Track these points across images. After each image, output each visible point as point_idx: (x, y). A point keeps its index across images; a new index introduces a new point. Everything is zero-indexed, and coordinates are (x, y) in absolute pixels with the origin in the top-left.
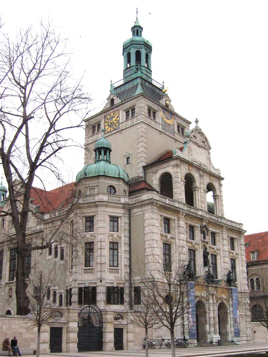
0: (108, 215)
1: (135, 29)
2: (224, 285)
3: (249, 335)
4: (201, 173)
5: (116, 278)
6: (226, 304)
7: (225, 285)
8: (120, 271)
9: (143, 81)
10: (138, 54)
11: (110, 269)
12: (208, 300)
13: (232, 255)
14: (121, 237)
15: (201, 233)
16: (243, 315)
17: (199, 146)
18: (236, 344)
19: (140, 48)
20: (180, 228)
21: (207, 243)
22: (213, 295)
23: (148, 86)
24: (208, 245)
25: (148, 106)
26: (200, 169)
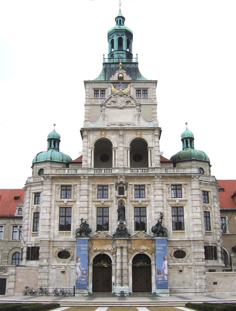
0: (33, 193)
1: (119, 19)
2: (144, 237)
3: (198, 287)
4: (121, 133)
5: (36, 239)
6: (149, 255)
7: (145, 236)
8: (39, 234)
10: (120, 40)
11: (32, 233)
13: (175, 203)
14: (40, 208)
15: (116, 190)
16: (192, 265)
17: (121, 108)
18: (158, 296)
19: (113, 37)
20: (82, 191)
21: (125, 198)
22: (122, 248)
24: (128, 200)
25: (94, 89)
26: (118, 129)
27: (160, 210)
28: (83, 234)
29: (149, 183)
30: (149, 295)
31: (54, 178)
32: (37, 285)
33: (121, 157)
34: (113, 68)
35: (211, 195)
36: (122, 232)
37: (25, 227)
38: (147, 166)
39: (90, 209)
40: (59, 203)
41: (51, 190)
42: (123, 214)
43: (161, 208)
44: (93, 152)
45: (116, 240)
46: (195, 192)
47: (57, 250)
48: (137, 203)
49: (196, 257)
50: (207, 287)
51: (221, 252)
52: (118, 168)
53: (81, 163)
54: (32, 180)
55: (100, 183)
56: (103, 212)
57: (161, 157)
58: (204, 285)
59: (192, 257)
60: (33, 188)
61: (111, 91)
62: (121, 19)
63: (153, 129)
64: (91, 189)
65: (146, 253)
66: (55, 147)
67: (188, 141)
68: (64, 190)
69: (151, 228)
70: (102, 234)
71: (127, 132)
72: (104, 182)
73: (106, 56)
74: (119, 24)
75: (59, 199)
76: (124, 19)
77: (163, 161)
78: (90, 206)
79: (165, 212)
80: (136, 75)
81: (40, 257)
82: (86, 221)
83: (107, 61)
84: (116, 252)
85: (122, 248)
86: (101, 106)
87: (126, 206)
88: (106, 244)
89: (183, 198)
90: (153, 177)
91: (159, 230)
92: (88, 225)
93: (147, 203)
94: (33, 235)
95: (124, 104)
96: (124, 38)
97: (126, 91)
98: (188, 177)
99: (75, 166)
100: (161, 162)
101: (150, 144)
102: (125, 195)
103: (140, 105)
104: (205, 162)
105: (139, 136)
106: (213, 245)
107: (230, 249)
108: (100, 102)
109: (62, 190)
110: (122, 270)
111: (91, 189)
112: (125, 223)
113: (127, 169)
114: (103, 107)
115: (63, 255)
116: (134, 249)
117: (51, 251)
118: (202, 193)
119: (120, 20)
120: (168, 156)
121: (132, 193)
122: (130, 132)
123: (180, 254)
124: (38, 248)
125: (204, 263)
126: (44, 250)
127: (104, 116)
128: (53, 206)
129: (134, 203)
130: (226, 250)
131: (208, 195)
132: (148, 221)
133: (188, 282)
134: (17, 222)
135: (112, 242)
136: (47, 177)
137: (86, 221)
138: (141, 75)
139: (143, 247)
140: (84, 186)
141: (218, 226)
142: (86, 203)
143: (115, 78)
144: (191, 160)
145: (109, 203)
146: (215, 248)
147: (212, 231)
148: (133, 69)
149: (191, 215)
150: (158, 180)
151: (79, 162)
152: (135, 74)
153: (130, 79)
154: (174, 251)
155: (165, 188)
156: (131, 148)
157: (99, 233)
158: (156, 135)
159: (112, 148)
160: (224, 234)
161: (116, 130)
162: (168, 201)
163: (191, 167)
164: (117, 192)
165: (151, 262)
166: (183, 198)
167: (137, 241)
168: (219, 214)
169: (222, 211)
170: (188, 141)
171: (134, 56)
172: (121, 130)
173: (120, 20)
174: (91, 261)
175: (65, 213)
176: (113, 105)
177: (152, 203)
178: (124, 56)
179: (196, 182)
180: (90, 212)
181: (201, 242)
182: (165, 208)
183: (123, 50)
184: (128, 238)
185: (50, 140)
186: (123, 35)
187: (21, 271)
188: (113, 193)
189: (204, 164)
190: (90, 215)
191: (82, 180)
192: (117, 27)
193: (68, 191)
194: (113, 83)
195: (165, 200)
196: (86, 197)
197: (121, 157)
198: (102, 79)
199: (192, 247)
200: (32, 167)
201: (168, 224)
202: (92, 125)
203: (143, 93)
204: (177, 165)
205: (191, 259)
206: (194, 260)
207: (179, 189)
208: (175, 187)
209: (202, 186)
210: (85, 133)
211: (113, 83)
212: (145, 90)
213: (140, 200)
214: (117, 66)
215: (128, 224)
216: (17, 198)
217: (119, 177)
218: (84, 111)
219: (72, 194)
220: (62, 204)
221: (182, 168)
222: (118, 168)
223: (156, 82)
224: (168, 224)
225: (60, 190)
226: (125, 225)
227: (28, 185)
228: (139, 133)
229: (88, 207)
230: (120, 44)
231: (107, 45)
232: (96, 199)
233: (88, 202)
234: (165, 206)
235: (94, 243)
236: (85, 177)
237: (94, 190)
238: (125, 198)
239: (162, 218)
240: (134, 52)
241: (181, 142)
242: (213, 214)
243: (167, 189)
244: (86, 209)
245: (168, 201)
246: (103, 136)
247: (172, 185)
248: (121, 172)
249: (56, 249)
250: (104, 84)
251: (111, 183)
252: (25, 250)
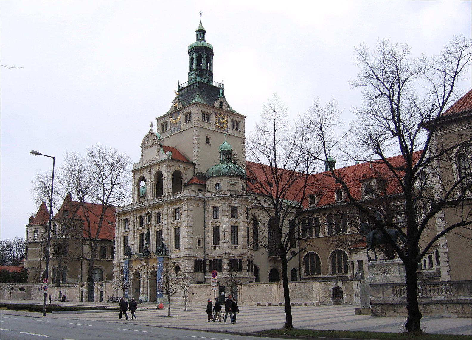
17: (150, 147)
22: (144, 266)
29: (162, 210)
106: (219, 258)
119: (201, 33)
159: (162, 179)
173: (201, 33)
180: (135, 239)
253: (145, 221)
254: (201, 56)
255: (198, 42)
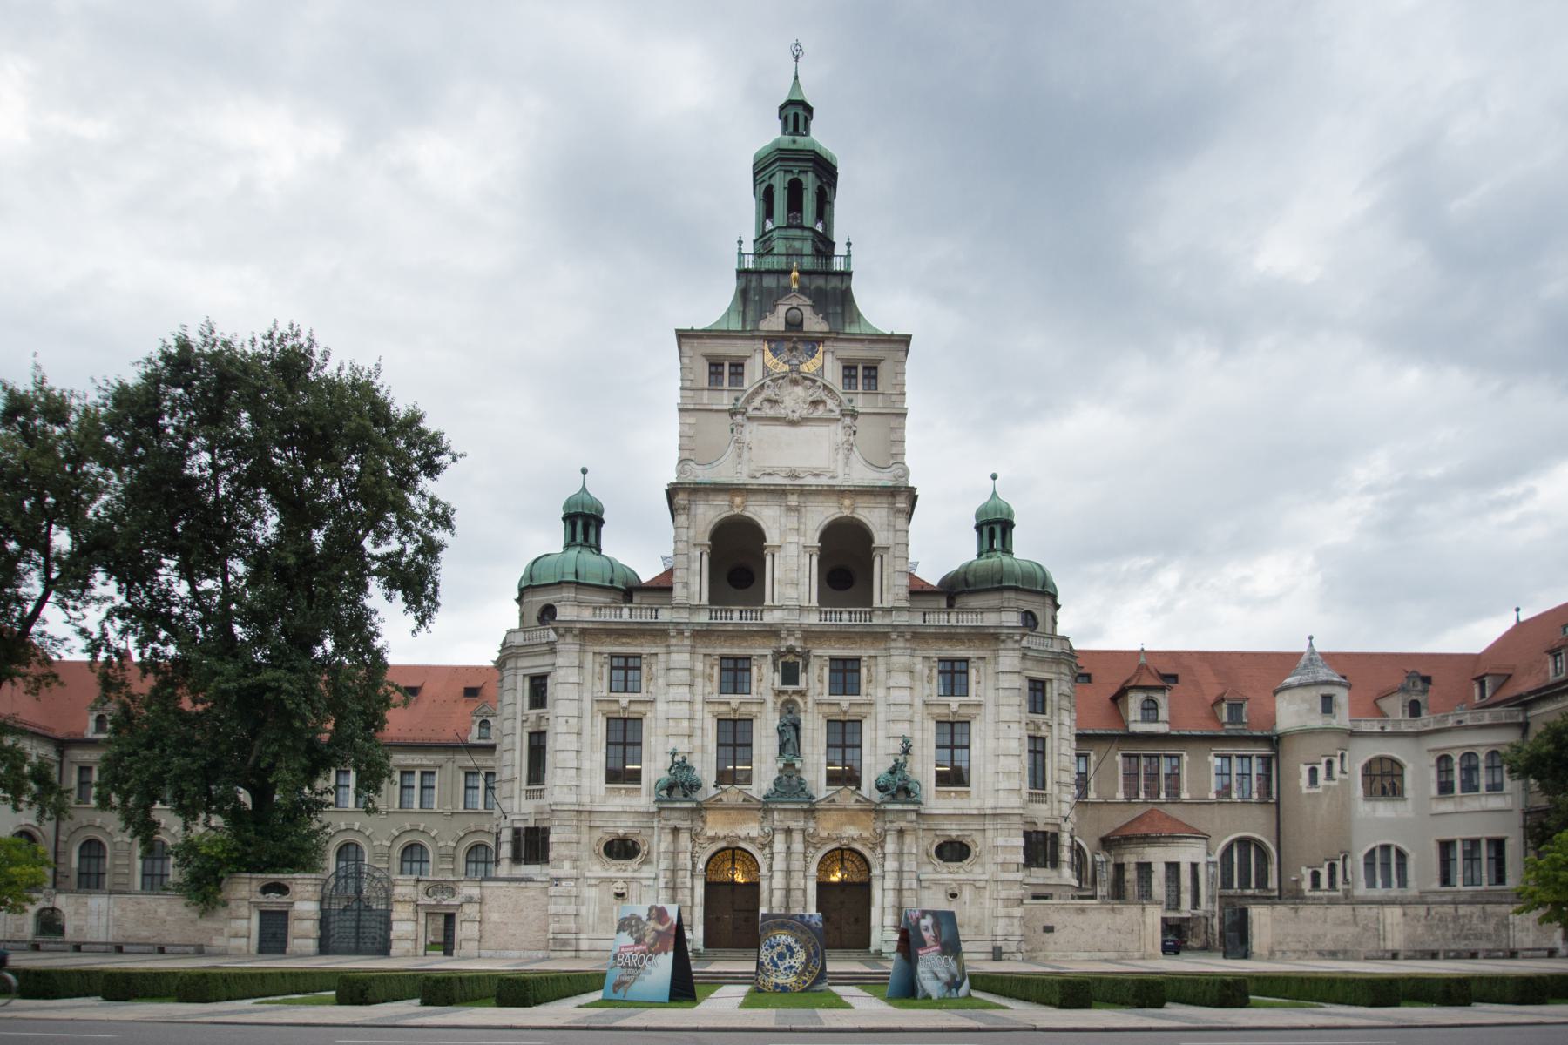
1: (791, 111)
4: (793, 500)
6: (867, 853)
9: (754, 277)
10: (795, 190)
12: (767, 844)
15: (776, 670)
20: (671, 673)
21: (802, 694)
23: (774, 284)
24: (810, 700)
25: (707, 357)
27: (903, 729)
28: (678, 793)
29: (872, 652)
30: (862, 956)
31: (587, 634)
32: (546, 931)
33: (791, 576)
34: (770, 290)
35: (1052, 692)
36: (790, 785)
37: (506, 774)
38: (869, 603)
39: (697, 724)
40: (606, 707)
41: (580, 667)
42: (793, 740)
43: (907, 725)
44: (705, 558)
45: (772, 810)
46: (1005, 681)
47: (600, 837)
48: (835, 709)
49: (1000, 859)
50: (1025, 939)
51: (1071, 848)
52: (781, 608)
53: (670, 589)
54: (519, 639)
55: (726, 651)
56: (734, 736)
57: (912, 576)
58: (1018, 932)
59: (987, 858)
60: (523, 663)
61: (765, 366)
62: (801, 112)
63: (891, 492)
64: (699, 666)
65: (857, 846)
66: (586, 538)
67: (995, 527)
68: (618, 668)
69: (873, 779)
70: (732, 794)
71: (811, 498)
72: (739, 646)
73: (748, 248)
74: (791, 129)
75: (605, 693)
76: (809, 110)
77: (918, 592)
78: (698, 716)
79: (917, 735)
80: (843, 313)
81: (552, 855)
82: (684, 760)
83: (749, 263)
84: (772, 842)
85: (788, 831)
86: (733, 413)
87: (802, 716)
88: (744, 821)
89: (972, 698)
90: (885, 636)
91: (898, 787)
92: (689, 768)
93: (864, 710)
94: (530, 795)
95: (803, 411)
96: (810, 182)
97: (809, 367)
98: (990, 638)
99: (651, 600)
100: (912, 593)
101: (879, 539)
102: (802, 686)
103: (854, 415)
104: (1043, 594)
105: (847, 513)
107: (1095, 841)
108: (725, 400)
109: (612, 668)
110: (788, 891)
111: (699, 666)
112: (798, 765)
113: (809, 609)
114: (739, 419)
115: (621, 849)
116: (824, 834)
117: (585, 838)
118: (1026, 685)
119: (796, 114)
120: (932, 575)
121: (821, 681)
122: (821, 498)
123: (953, 851)
124: (546, 831)
125: (1020, 876)
126: (563, 838)
127: (741, 446)
128: (587, 715)
129: (826, 709)
130: (1083, 844)
131: (1043, 691)
132: (865, 761)
133: (974, 923)
134: (480, 760)
135: (760, 815)
136: (566, 630)
137: (684, 760)
138: (859, 315)
139: (851, 831)
140: (681, 658)
141: (1069, 778)
142: (686, 706)
143: (775, 322)
144: (1001, 589)
145: (754, 709)
146: (1055, 836)
147: (1048, 790)
148: (834, 296)
149: (991, 744)
150: (901, 644)
151: (662, 588)
152: (839, 309)
153: (824, 327)
154: (937, 842)
155: (919, 667)
156: (821, 549)
157: (725, 791)
158: (899, 511)
160: (1081, 799)
161: (778, 492)
162: (926, 704)
163: (1000, 610)
164: (778, 677)
165: (869, 870)
166: (972, 698)
167: (834, 815)
168: (1074, 745)
169: (1081, 738)
170: (995, 527)
171: (839, 249)
172: (793, 492)
173: (796, 114)
174: (701, 866)
175: (624, 736)
176: (768, 411)
177: (881, 710)
178: (807, 248)
179: (1011, 653)
180: (699, 733)
181: (1017, 819)
182: (917, 725)
183: (802, 227)
184: (806, 806)
185: (570, 518)
186: (805, 172)
187: (498, 892)
188: (764, 679)
189: (1038, 599)
190: (697, 741)
191: (673, 641)
192: (787, 141)
193: (630, 673)
194: (770, 339)
195: (918, 702)
196: (686, 689)
197: (791, 576)
198: (735, 325)
199: (990, 834)
200: (519, 600)
201: (924, 769)
202: (703, 475)
203: (865, 377)
204: (959, 602)
205: (983, 865)
206: (994, 868)
207: (961, 672)
208: (948, 667)
209: (1029, 664)
210: (681, 499)
211: (770, 339)
212: (875, 365)
213: (845, 701)
214: (784, 281)
215: (808, 767)
216: (471, 692)
217: (783, 634)
218: (677, 428)
219: (644, 680)
220: (614, 707)
221: (972, 611)
222: (781, 608)
223: (905, 341)
224: (924, 769)
225: (606, 668)
226: (799, 771)
227: (509, 652)
228: (847, 502)
229: (691, 719)
230: (795, 204)
231: (749, 205)
232: (716, 695)
233: (691, 703)
234: (917, 718)
235: (710, 817)
236: (680, 632)
237: (708, 670)
238: (802, 694)
239: (906, 752)
240: (839, 237)
241: (975, 534)
242: (1056, 744)
243: (926, 672)
244: (685, 723)
245: (926, 704)
246: (737, 511)
247: (941, 660)
248: (791, 618)
249: (598, 834)
250: (739, 342)
251: (761, 650)
252: (506, 835)
253: (764, 679)
254: (797, 181)
255: (788, 138)
